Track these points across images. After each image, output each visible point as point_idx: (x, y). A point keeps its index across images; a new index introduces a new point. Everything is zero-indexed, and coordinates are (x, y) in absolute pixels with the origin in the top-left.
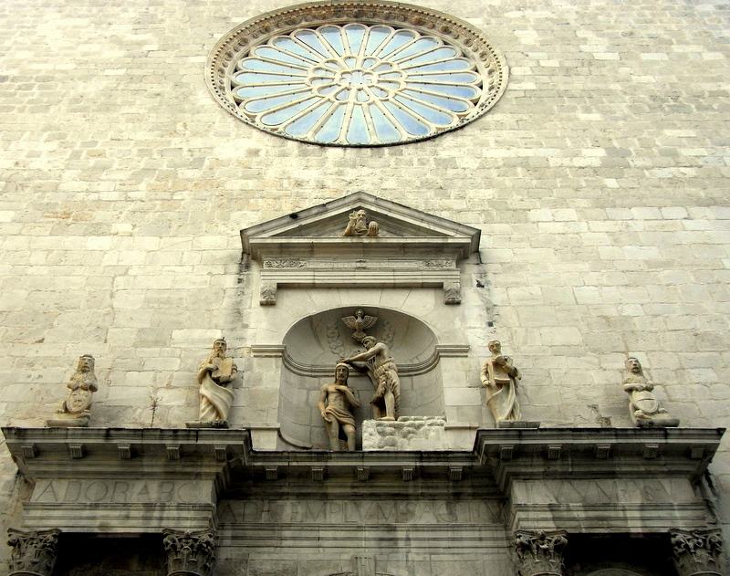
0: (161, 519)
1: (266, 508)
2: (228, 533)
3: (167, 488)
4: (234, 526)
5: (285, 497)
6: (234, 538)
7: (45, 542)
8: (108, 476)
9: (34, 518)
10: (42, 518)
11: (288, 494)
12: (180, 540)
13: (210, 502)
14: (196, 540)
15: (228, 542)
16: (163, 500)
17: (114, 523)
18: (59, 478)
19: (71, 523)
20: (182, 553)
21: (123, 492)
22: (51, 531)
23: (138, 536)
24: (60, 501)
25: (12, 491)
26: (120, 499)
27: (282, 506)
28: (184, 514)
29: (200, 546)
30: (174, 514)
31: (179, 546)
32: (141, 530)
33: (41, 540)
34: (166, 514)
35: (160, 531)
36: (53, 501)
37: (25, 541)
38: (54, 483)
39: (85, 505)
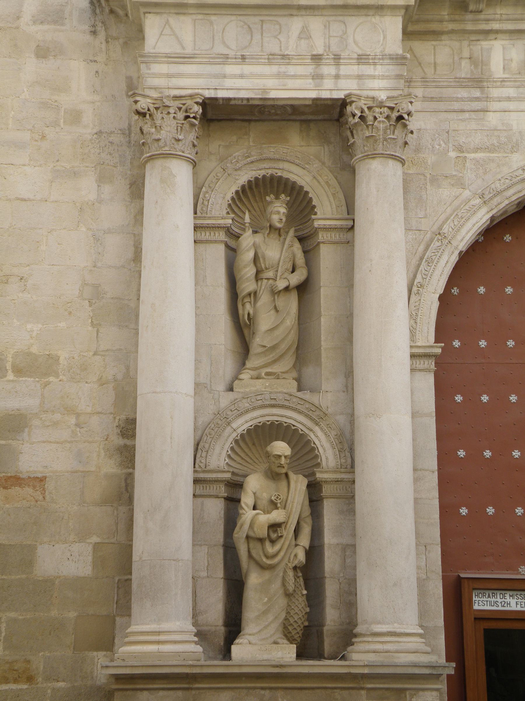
0: (337, 77)
1: (466, 54)
2: (419, 92)
3: (336, 28)
4: (425, 81)
5: (492, 36)
6: (425, 99)
7: (186, 111)
8: (249, 11)
9: (160, 75)
10: (169, 76)
11: (497, 32)
12: (370, 108)
13: (400, 52)
14: (392, 109)
15: (417, 105)
16: (335, 49)
17: (270, 83)
18: (177, 14)
19: (215, 83)
20: (378, 129)
21: (276, 37)
22: (191, 96)
23: (310, 103)
24: (189, 50)
25: (94, 26)
26: (272, 46)
27: (489, 50)
28: (368, 70)
29: (400, 118)
30: (354, 69)
31: (370, 118)
32: (313, 95)
33: (180, 109)
34: (344, 70)
35: (341, 95)
36: (179, 50)
37: (157, 108)
38: (173, 20)
39: (226, 57)
